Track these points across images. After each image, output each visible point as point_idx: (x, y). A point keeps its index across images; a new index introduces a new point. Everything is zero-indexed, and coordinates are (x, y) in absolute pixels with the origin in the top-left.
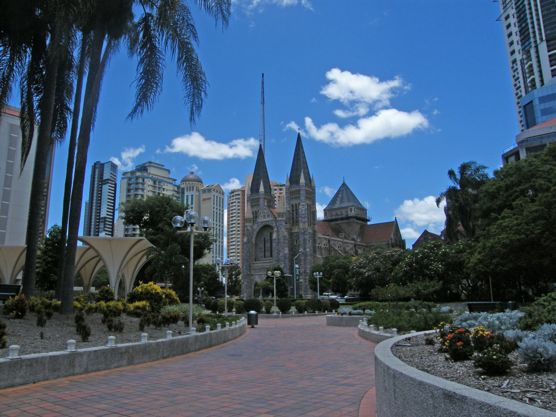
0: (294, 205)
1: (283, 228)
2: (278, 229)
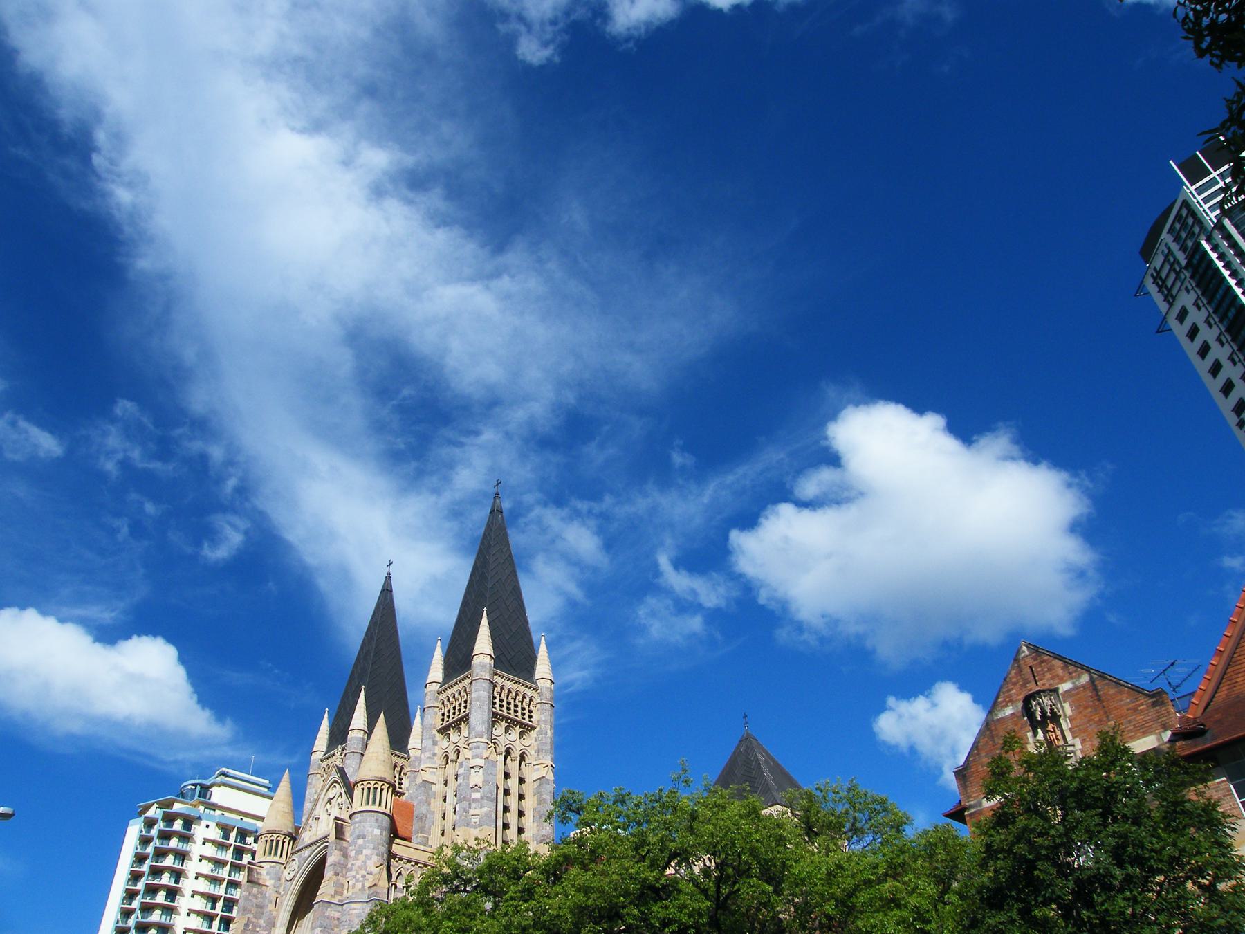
2: (345, 856)
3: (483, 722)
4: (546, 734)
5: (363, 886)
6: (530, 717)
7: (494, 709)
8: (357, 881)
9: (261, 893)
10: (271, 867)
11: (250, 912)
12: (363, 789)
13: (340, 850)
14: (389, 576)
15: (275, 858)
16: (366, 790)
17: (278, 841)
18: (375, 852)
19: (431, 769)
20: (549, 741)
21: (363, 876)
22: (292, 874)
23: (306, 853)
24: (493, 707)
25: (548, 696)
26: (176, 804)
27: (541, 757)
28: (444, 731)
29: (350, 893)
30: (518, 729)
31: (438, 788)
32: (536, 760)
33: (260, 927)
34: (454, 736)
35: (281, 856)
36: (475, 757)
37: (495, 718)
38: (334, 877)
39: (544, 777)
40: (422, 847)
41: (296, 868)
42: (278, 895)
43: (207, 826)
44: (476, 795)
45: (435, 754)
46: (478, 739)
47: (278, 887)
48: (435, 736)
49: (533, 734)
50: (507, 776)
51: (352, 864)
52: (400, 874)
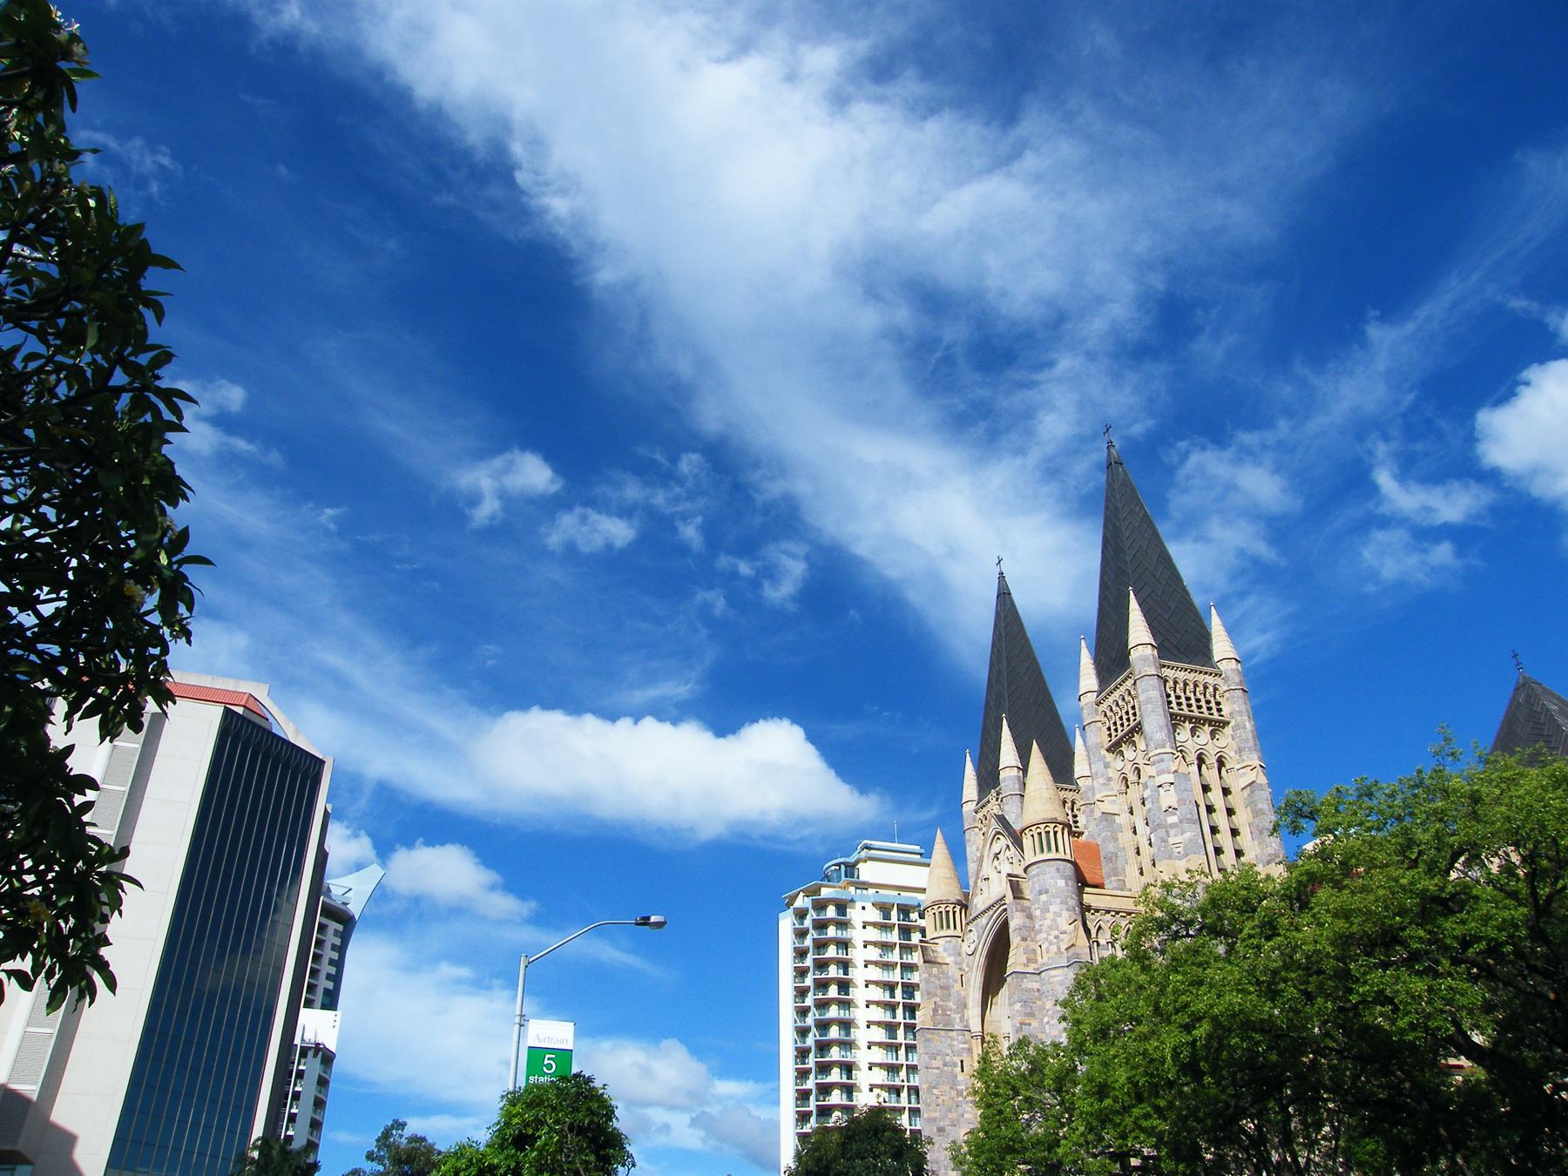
1: (1053, 908)
2: (1030, 917)
3: (1161, 728)
4: (1244, 727)
5: (1059, 948)
6: (1219, 710)
7: (1171, 710)
9: (943, 973)
11: (935, 995)
12: (1032, 836)
14: (1001, 576)
15: (948, 931)
16: (1036, 836)
17: (948, 912)
18: (1064, 907)
20: (1250, 736)
22: (973, 947)
23: (983, 920)
24: (1169, 708)
25: (1237, 679)
26: (822, 889)
28: (1115, 748)
29: (1045, 959)
30: (1207, 729)
31: (1123, 819)
32: (1239, 763)
33: (951, 1010)
34: (1129, 753)
35: (955, 928)
36: (1160, 773)
37: (1175, 721)
38: (1024, 944)
39: (1253, 782)
40: (1119, 893)
41: (976, 939)
42: (962, 973)
43: (863, 908)
44: (1173, 819)
45: (1110, 779)
47: (960, 964)
48: (1104, 756)
49: (1228, 730)
50: (1206, 789)
51: (1041, 925)
52: (1100, 928)
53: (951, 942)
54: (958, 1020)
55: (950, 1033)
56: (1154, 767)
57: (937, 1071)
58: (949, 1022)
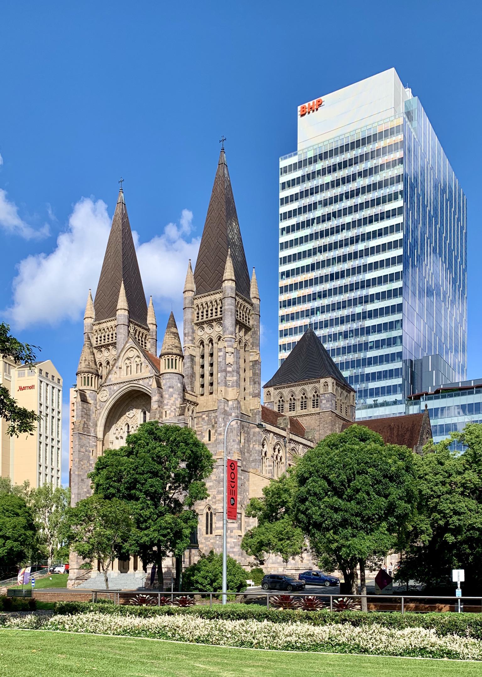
0: (206, 342)
1: (175, 396)
2: (162, 397)
8: (172, 411)
10: (91, 393)
12: (165, 360)
13: (160, 393)
19: (193, 348)
21: (175, 409)
22: (105, 399)
23: (115, 388)
27: (255, 348)
28: (200, 325)
29: (168, 418)
31: (198, 359)
36: (229, 346)
40: (193, 394)
44: (229, 369)
46: (230, 336)
47: (96, 404)
49: (250, 333)
53: (92, 393)
54: (93, 431)
55: (89, 437)
56: (226, 343)
57: (83, 453)
58: (89, 432)
